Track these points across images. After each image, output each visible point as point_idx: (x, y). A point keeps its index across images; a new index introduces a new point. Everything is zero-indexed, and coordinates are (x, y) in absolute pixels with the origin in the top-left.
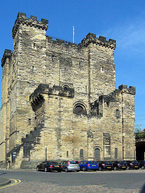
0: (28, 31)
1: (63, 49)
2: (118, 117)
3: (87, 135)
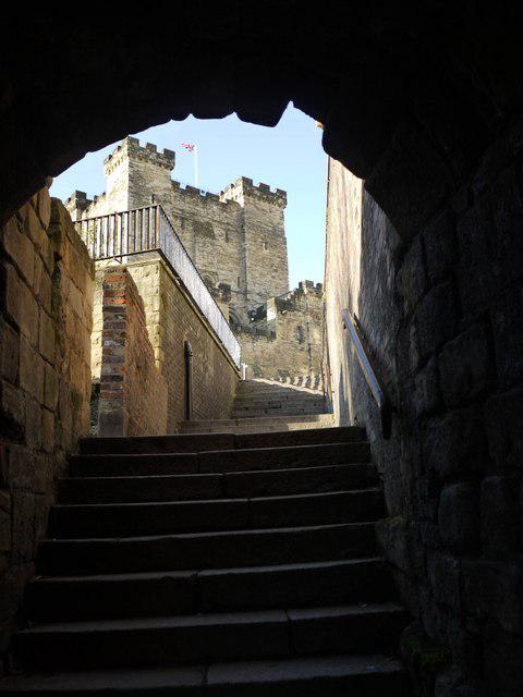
2: (301, 341)
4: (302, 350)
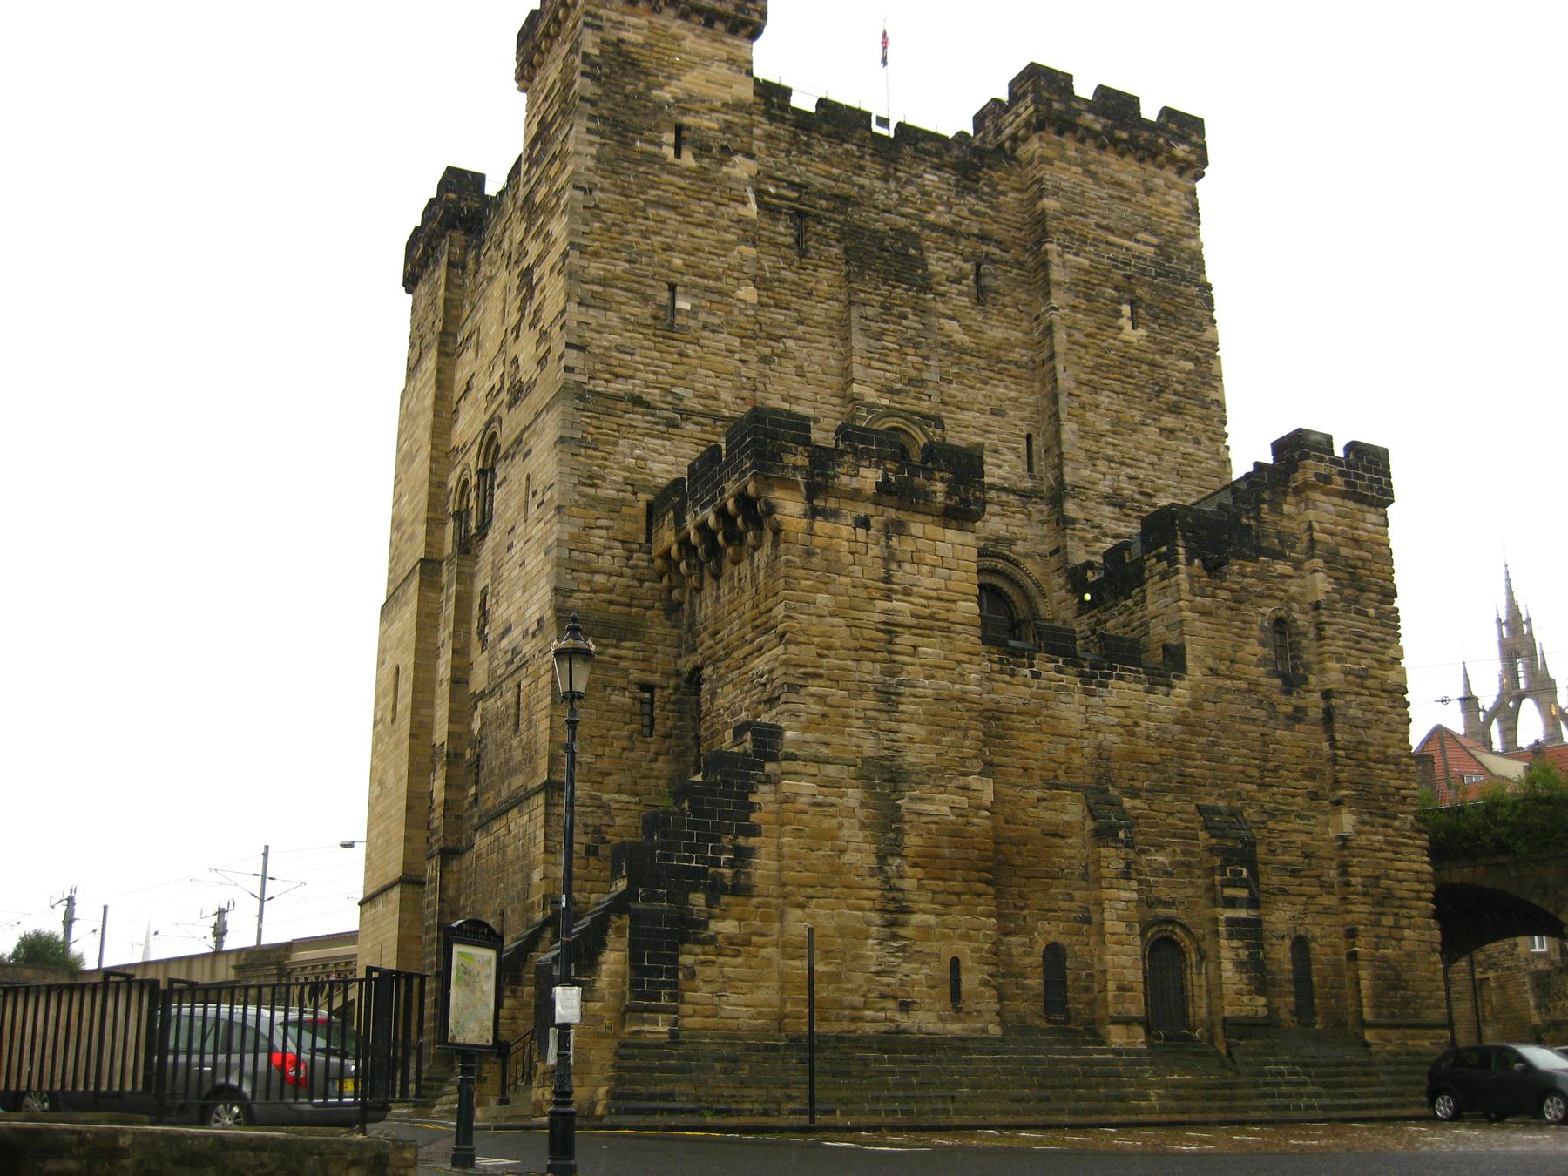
0: (640, 39)
1: (862, 168)
2: (1292, 682)
3: (1090, 825)
4: (1298, 715)
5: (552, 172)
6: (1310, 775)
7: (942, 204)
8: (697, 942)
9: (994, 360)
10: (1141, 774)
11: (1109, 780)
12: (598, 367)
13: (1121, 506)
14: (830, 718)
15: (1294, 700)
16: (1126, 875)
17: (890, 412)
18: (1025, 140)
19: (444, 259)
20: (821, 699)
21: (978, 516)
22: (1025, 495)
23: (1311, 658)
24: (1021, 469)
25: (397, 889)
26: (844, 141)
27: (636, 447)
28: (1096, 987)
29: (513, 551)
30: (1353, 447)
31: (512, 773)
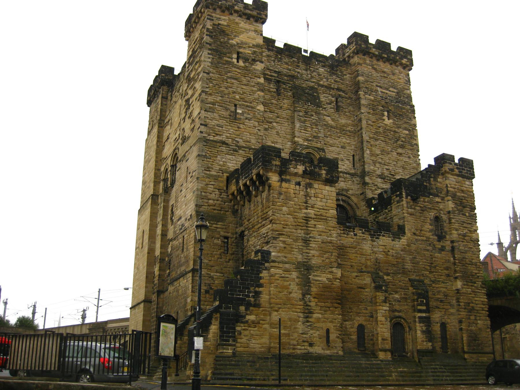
0: (225, 24)
1: (298, 66)
2: (441, 238)
3: (373, 285)
4: (442, 249)
5: (196, 67)
6: (447, 269)
7: (325, 79)
8: (242, 322)
9: (342, 130)
10: (390, 268)
11: (379, 270)
12: (211, 131)
13: (384, 179)
14: (287, 249)
15: (441, 244)
16: (385, 301)
17: (307, 147)
18: (353, 57)
19: (160, 96)
20: (284, 242)
21: (337, 182)
22: (352, 175)
23: (447, 230)
24: (351, 166)
25: (143, 304)
26: (292, 57)
27: (223, 158)
28: (375, 339)
29: (182, 192)
30: (461, 160)
31: (181, 266)
